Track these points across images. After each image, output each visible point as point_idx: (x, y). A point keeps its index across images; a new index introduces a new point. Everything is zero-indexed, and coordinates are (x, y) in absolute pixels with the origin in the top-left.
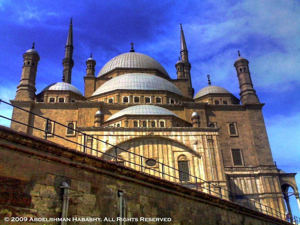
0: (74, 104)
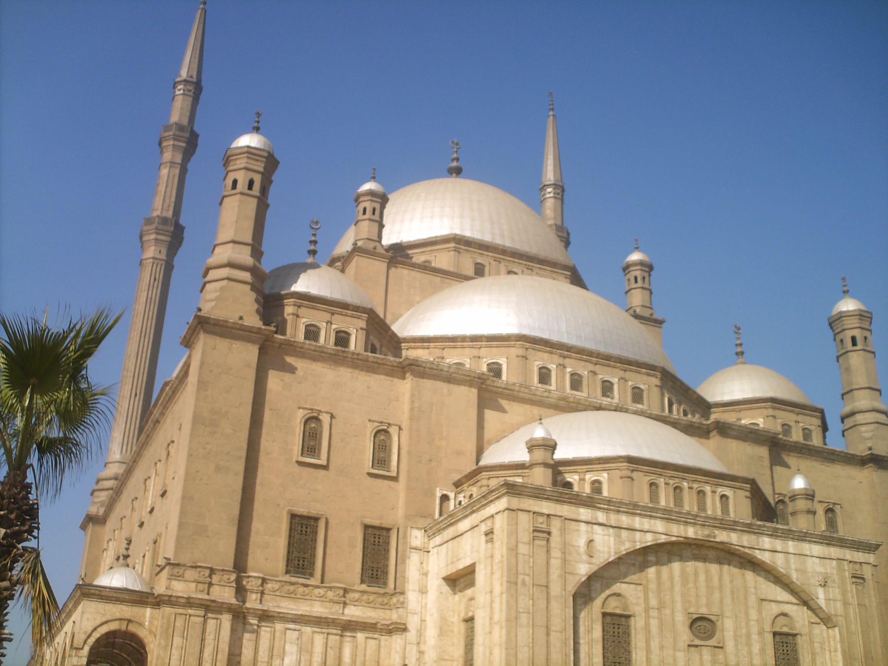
0: (395, 364)
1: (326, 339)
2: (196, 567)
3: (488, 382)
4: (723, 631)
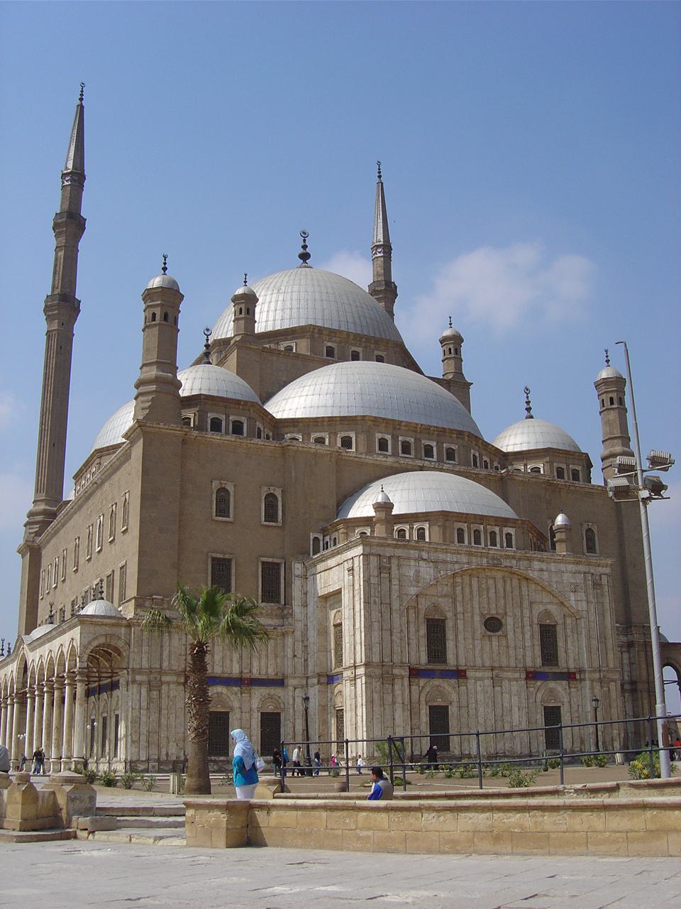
2: (153, 599)
3: (343, 454)
4: (506, 625)
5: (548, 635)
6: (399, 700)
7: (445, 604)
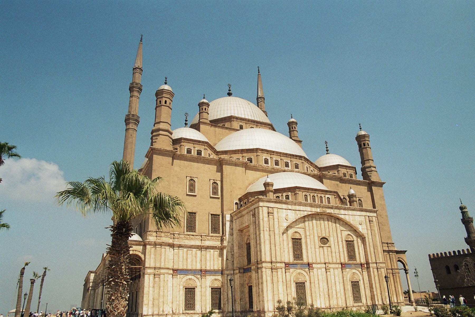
1: (194, 153)
5: (350, 245)
6: (280, 280)
7: (301, 231)
